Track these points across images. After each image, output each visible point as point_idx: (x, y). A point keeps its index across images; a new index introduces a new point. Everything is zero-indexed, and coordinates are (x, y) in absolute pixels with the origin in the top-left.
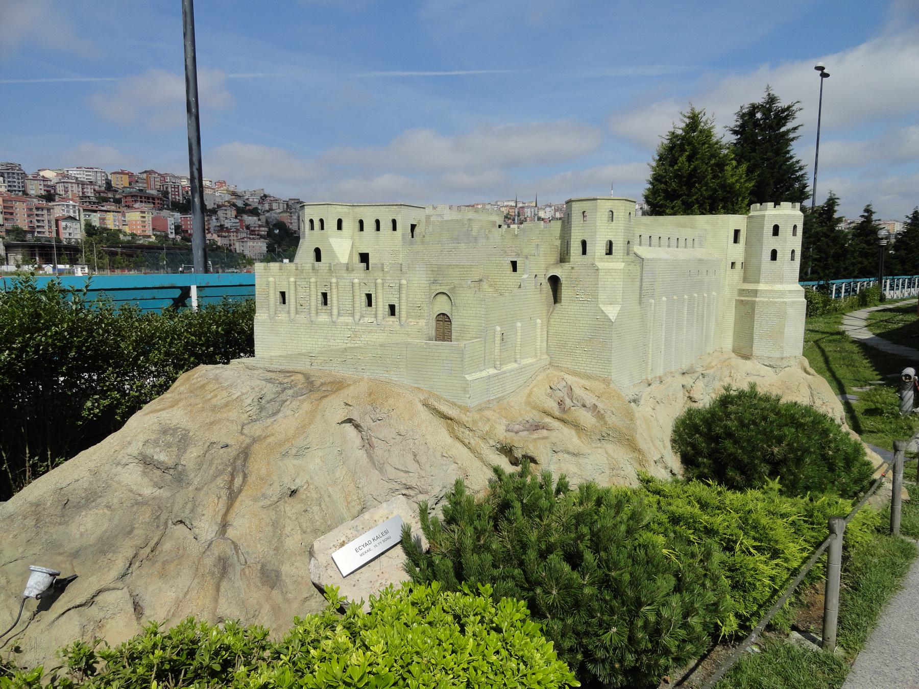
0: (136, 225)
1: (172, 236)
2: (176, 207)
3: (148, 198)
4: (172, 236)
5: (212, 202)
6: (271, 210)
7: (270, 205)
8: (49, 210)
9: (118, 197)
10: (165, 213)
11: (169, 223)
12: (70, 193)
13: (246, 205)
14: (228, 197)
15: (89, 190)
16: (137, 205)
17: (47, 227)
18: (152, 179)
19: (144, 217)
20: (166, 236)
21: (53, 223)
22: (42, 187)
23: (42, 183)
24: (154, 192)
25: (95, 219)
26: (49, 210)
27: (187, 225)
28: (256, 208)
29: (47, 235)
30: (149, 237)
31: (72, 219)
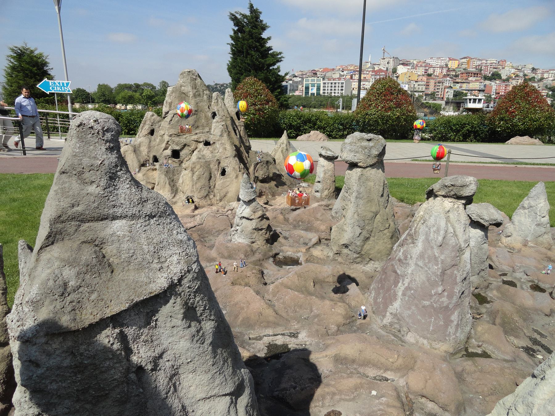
2: (486, 78)
3: (475, 74)
4: (493, 96)
5: (505, 74)
7: (543, 73)
8: (443, 83)
10: (487, 82)
11: (493, 88)
12: (435, 73)
13: (525, 75)
14: (513, 71)
16: (470, 79)
20: (490, 95)
24: (474, 70)
27: (500, 89)
28: (534, 77)
29: (439, 96)
31: (451, 87)
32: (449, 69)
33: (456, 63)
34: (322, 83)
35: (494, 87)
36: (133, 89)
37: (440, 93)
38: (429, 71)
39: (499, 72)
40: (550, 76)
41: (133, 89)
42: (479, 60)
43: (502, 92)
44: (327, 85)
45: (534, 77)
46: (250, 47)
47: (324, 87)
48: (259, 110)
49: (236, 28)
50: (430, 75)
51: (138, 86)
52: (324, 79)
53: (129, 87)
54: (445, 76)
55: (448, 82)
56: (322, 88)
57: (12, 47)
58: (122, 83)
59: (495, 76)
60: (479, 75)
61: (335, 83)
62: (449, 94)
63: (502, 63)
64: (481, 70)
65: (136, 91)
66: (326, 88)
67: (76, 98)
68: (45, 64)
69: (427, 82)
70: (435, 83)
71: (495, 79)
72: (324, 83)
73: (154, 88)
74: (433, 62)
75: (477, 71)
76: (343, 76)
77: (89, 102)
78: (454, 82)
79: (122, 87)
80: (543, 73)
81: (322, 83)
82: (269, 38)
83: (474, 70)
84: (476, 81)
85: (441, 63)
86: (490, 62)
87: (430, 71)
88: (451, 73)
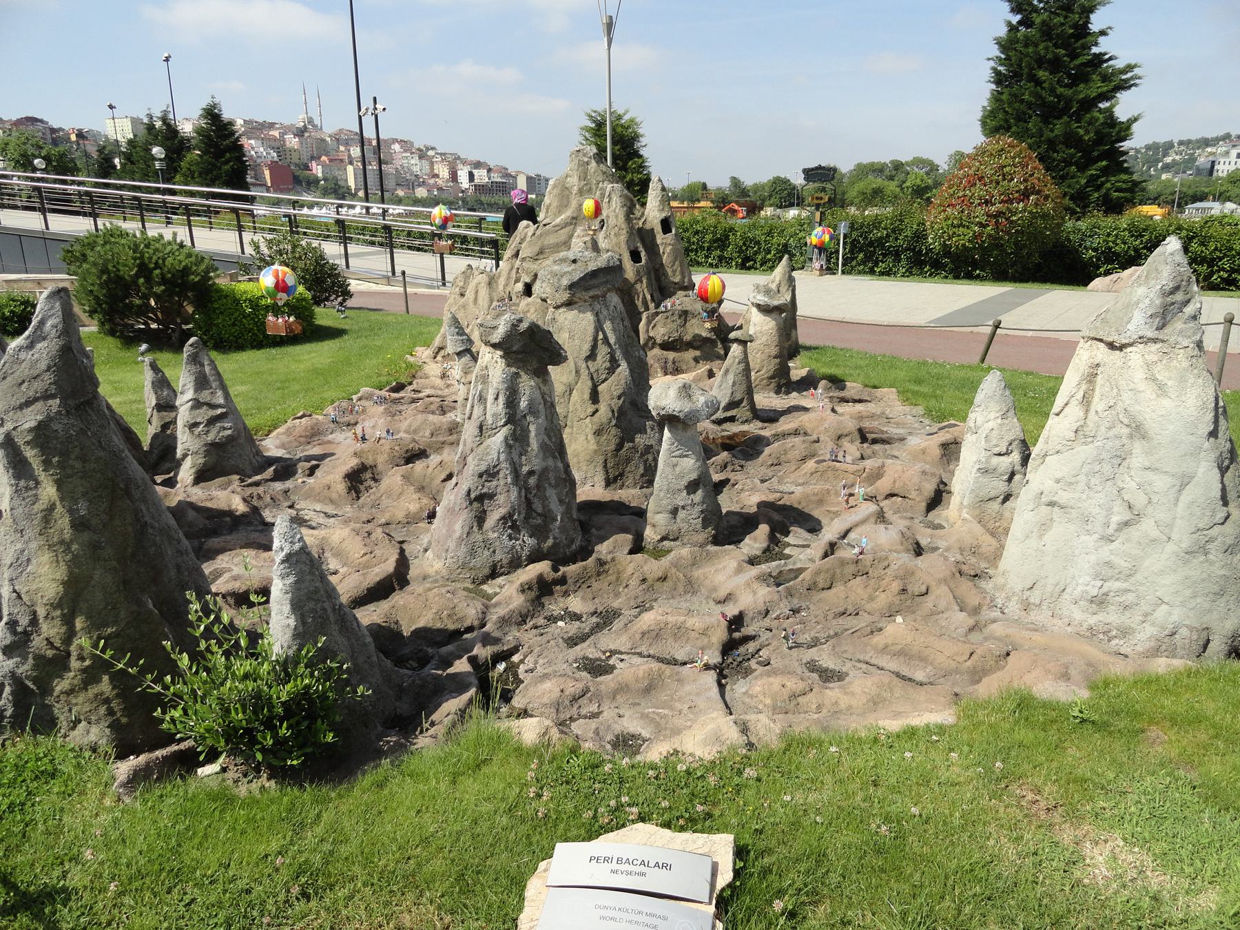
36: (887, 172)
41: (887, 172)
46: (1041, 62)
48: (1000, 214)
49: (1015, 19)
51: (898, 166)
53: (878, 169)
57: (589, 111)
58: (866, 160)
65: (891, 178)
67: (770, 196)
68: (636, 137)
73: (933, 168)
77: (791, 205)
79: (864, 171)
82: (1103, 33)
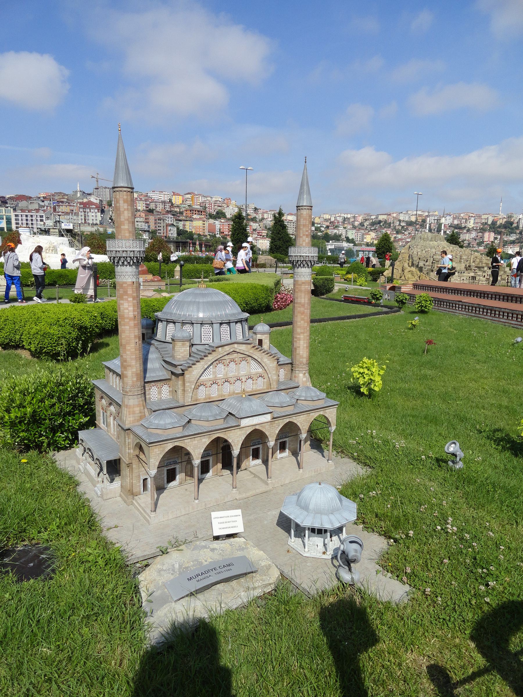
0: (200, 228)
1: (218, 236)
2: (211, 216)
3: (199, 211)
4: (218, 236)
5: (230, 213)
6: (263, 219)
7: (263, 214)
8: (163, 220)
9: (181, 210)
10: (211, 221)
11: (217, 228)
12: (158, 208)
15: (167, 207)
16: (195, 216)
17: (162, 230)
18: (196, 199)
19: (204, 224)
20: (215, 235)
21: (165, 227)
22: (144, 205)
23: (144, 202)
24: (198, 207)
25: (181, 225)
26: (163, 220)
28: (255, 217)
29: (162, 234)
30: (206, 236)
31: (173, 225)
32: (172, 204)
33: (181, 198)
34: (12, 215)
35: (218, 227)
37: (162, 232)
38: (151, 206)
39: (224, 211)
40: (269, 217)
42: (204, 196)
43: (226, 231)
44: (20, 218)
45: (255, 217)
47: (16, 220)
50: (151, 211)
52: (15, 210)
54: (168, 212)
55: (170, 219)
56: (13, 222)
59: (220, 215)
60: (203, 213)
61: (32, 216)
62: (172, 232)
63: (227, 201)
64: (206, 208)
66: (20, 222)
69: (146, 219)
70: (156, 220)
71: (220, 218)
72: (16, 216)
74: (155, 196)
75: (201, 209)
76: (44, 207)
78: (176, 220)
80: (263, 214)
81: (12, 215)
83: (198, 207)
84: (200, 219)
85: (164, 197)
86: (216, 199)
87: (152, 206)
88: (176, 210)
